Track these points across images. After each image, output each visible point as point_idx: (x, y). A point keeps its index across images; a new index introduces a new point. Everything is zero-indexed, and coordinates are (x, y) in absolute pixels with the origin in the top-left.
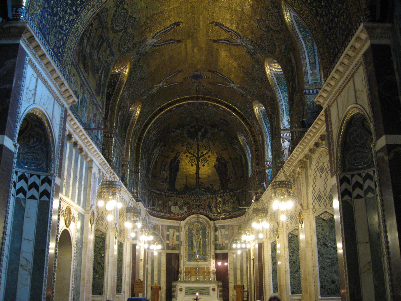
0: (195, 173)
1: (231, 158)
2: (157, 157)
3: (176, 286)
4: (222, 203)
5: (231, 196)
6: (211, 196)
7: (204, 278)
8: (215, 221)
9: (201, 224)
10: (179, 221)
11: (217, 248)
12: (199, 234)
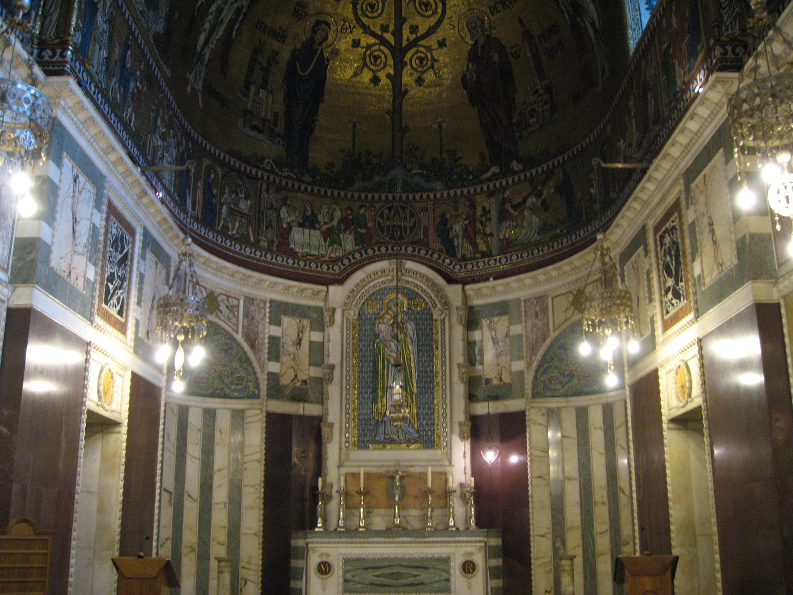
0: (388, 112)
1: (527, 35)
2: (233, 21)
3: (303, 552)
4: (494, 214)
5: (532, 181)
6: (452, 193)
7: (424, 518)
8: (468, 287)
9: (409, 299)
10: (324, 288)
11: (480, 392)
12: (401, 337)
